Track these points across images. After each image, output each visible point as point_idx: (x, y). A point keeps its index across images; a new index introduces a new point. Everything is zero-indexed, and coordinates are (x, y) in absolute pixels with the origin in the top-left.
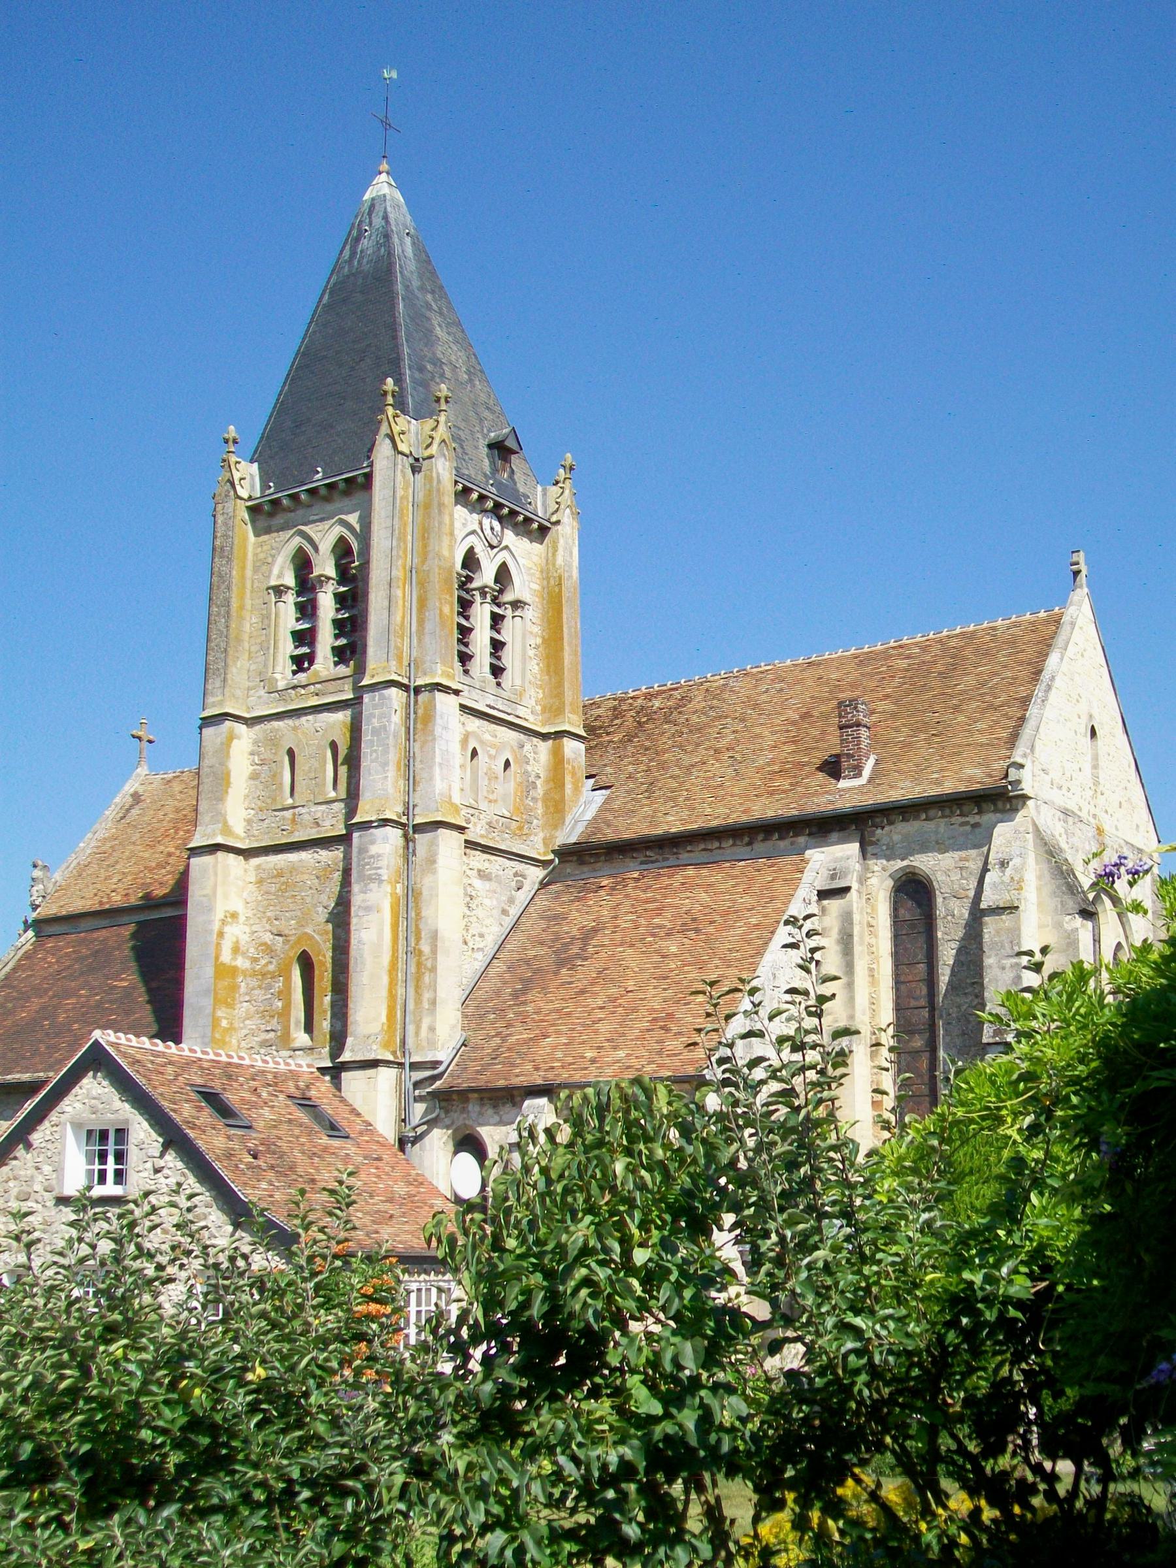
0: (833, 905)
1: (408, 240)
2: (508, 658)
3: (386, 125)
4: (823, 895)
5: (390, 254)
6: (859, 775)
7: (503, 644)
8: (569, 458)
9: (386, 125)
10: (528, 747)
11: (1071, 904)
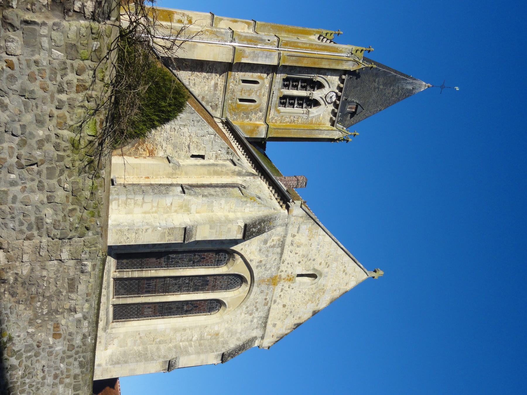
1: (410, 87)
2: (289, 109)
3: (442, 87)
5: (407, 76)
7: (293, 107)
9: (442, 87)
10: (260, 114)
11: (248, 222)
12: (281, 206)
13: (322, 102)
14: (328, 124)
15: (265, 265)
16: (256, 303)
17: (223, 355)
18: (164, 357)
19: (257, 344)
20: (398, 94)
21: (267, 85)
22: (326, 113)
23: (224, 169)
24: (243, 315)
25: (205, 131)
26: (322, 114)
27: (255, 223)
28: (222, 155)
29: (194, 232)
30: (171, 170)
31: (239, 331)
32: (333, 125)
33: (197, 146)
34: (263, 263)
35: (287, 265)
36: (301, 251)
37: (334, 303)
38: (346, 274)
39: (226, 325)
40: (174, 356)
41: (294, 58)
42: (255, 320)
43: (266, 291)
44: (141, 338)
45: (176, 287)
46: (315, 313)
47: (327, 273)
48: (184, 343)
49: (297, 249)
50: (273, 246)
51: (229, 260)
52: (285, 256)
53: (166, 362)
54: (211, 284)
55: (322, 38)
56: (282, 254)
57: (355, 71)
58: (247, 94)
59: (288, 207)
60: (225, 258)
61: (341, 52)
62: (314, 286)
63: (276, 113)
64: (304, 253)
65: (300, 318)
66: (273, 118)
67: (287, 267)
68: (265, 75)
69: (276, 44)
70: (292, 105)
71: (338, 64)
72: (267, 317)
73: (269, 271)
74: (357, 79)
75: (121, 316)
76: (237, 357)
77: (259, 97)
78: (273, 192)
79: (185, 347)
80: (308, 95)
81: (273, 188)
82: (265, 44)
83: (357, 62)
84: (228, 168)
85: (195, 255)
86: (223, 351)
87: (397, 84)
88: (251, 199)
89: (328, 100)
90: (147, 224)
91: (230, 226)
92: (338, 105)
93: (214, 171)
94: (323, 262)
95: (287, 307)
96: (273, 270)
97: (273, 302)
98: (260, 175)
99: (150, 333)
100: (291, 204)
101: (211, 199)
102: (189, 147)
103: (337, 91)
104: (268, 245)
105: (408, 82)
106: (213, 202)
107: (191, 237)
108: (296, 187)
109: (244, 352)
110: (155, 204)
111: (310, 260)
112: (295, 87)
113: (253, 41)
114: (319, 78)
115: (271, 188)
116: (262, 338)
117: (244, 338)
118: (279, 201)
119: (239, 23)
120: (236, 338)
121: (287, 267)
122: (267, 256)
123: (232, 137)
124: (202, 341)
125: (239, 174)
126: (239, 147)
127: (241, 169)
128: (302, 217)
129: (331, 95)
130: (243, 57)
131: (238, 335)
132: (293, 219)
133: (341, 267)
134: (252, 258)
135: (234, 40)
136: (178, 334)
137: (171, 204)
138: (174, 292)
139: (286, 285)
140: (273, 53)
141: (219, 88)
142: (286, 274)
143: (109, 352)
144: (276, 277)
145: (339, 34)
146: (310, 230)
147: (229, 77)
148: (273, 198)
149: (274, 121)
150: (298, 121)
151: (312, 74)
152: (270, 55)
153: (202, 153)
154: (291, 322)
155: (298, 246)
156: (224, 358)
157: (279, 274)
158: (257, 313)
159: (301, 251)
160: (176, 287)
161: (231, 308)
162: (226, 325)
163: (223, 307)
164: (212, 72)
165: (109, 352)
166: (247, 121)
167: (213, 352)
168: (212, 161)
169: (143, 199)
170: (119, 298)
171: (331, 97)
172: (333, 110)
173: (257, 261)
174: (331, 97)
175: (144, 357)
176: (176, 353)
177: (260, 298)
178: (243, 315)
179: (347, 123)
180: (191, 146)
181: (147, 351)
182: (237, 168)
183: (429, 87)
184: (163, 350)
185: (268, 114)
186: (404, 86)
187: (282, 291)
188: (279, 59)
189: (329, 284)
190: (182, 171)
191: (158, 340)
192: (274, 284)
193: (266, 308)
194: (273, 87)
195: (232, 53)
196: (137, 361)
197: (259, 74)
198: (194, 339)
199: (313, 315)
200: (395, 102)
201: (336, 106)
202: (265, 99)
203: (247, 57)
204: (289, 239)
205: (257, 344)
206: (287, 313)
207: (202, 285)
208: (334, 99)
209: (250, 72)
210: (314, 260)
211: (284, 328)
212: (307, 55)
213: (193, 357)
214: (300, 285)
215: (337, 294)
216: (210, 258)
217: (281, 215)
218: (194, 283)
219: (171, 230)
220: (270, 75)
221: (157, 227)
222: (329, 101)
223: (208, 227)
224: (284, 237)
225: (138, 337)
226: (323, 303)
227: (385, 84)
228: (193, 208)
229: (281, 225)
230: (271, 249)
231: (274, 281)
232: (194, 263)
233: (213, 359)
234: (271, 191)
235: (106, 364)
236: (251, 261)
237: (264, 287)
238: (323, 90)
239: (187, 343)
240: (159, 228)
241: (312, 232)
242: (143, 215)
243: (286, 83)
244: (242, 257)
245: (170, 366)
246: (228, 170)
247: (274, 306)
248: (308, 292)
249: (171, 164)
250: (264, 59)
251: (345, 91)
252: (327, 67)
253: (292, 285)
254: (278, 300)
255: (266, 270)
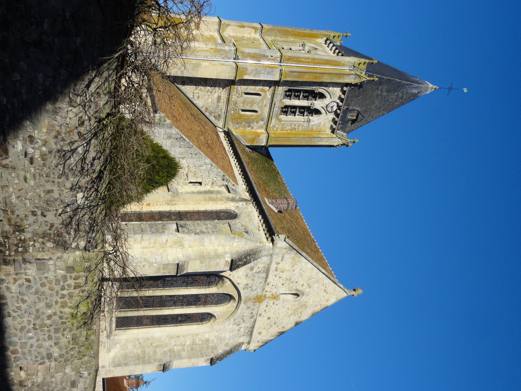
0: (224, 189)
1: (416, 91)
2: (290, 117)
3: (450, 89)
4: (227, 187)
5: (413, 82)
6: (270, 203)
7: (295, 116)
8: (356, 141)
9: (450, 89)
10: (262, 123)
11: (235, 257)
12: (267, 238)
13: (323, 111)
14: (329, 131)
15: (251, 287)
16: (243, 316)
17: (212, 359)
18: (160, 360)
19: (243, 347)
20: (402, 98)
21: (269, 97)
22: (327, 121)
23: (219, 196)
24: (231, 325)
25: (202, 162)
26: (323, 122)
27: (241, 258)
28: (217, 182)
29: (186, 266)
30: (170, 198)
31: (227, 338)
32: (333, 131)
33: (195, 174)
34: (250, 285)
35: (271, 286)
36: (284, 275)
37: (314, 315)
38: (327, 293)
39: (216, 334)
40: (168, 360)
41: (295, 74)
42: (242, 330)
43: (252, 307)
44: (140, 343)
45: (172, 303)
46: (297, 324)
47: (309, 292)
48: (178, 347)
49: (281, 274)
50: (259, 272)
51: (218, 281)
52: (270, 279)
53: (161, 365)
54: (203, 300)
55: (328, 42)
56: (267, 278)
57: (357, 84)
58: (249, 105)
59: (273, 241)
60: (215, 280)
61: (344, 65)
62: (296, 303)
63: (277, 122)
64: (288, 277)
65: (283, 327)
66: (274, 126)
67: (272, 288)
68: (267, 88)
69: (279, 59)
70: (294, 113)
71: (340, 78)
72: (253, 327)
73: (255, 292)
74: (359, 89)
75: (123, 325)
76: (225, 360)
77: (261, 107)
78: (262, 221)
79: (179, 351)
80: (309, 105)
81: (262, 218)
82: (268, 60)
83: (358, 75)
84: (223, 195)
85: (188, 278)
86: (212, 356)
87: (402, 90)
88: (239, 236)
89: (329, 109)
90: (145, 260)
91: (218, 260)
92: (339, 114)
93: (209, 198)
94: (305, 283)
95: (271, 319)
96: (258, 290)
97: (258, 315)
98: (252, 200)
99: (148, 339)
100: (275, 238)
101: (202, 236)
102: (187, 176)
103: (338, 101)
104: (254, 271)
105: (413, 86)
106: (204, 239)
107: (183, 270)
108: (287, 210)
109: (232, 354)
110: (152, 241)
111: (293, 282)
112: (298, 97)
113: (256, 58)
114: (321, 90)
115: (260, 217)
116: (249, 343)
117: (232, 343)
118: (266, 232)
119: (246, 28)
120: (224, 343)
121: (272, 288)
122: (253, 280)
123: (232, 151)
124: (194, 346)
125: (233, 200)
126: (237, 165)
127: (235, 196)
128: (286, 249)
129: (332, 105)
130: (246, 74)
131: (227, 341)
132: (277, 250)
133: (322, 288)
134: (239, 282)
135: (238, 57)
136: (173, 340)
137: (167, 241)
138: (170, 306)
139: (271, 302)
140: (275, 70)
141: (222, 100)
142: (271, 293)
143: (112, 354)
144: (261, 296)
145: (347, 36)
146: (293, 259)
147: (232, 90)
148: (261, 229)
149: (275, 129)
150: (298, 128)
151: (313, 86)
152: (272, 71)
153: (200, 180)
154: (275, 331)
155: (282, 272)
156: (212, 362)
157: (264, 293)
158: (243, 324)
159: (284, 275)
160: (172, 303)
161: (221, 320)
162: (216, 334)
163: (213, 319)
164: (215, 86)
165: (112, 354)
166: (248, 129)
167: (203, 357)
168: (208, 188)
169: (142, 237)
170: (121, 311)
171: (332, 107)
172: (334, 119)
173: (244, 284)
174: (332, 107)
175: (142, 359)
176: (170, 357)
177: (247, 313)
178: (231, 325)
179: (348, 129)
180: (189, 175)
181: (145, 354)
182: (231, 195)
183: (435, 89)
184: (159, 354)
185: (269, 123)
186: (409, 91)
187: (267, 306)
188: (281, 75)
189: (311, 301)
190: (180, 199)
191: (155, 344)
192: (259, 302)
193: (252, 320)
194: (275, 98)
195: (234, 71)
196: (136, 364)
197: (261, 87)
198: (187, 344)
199: (295, 325)
200: (398, 106)
201: (337, 115)
202: (267, 109)
203: (249, 74)
204: (273, 266)
205: (243, 347)
206: (271, 324)
207: (195, 301)
208: (335, 108)
209: (253, 85)
210: (297, 282)
211: (269, 335)
212: (309, 71)
213: (185, 361)
214: (283, 302)
215: (318, 308)
216: (202, 280)
217: (267, 247)
218: (187, 300)
219: (166, 266)
220: (272, 88)
221: (153, 263)
222: (330, 111)
223: (198, 262)
224: (269, 265)
225: (137, 342)
226: (305, 316)
227: (388, 91)
228: (186, 244)
229: (266, 255)
230: (257, 275)
231: (259, 299)
232: (187, 284)
233: (203, 362)
234: (260, 220)
235: (109, 365)
236: (238, 284)
237: (250, 304)
238: (325, 100)
239: (181, 348)
240: (155, 264)
241: (294, 260)
242: (142, 250)
243: (288, 93)
244: (230, 280)
245: (165, 368)
246: (222, 197)
247: (259, 318)
248: (290, 307)
249: (170, 193)
250: (266, 76)
251: (346, 101)
252: (328, 81)
253: (276, 302)
254: (263, 314)
255: (252, 290)
